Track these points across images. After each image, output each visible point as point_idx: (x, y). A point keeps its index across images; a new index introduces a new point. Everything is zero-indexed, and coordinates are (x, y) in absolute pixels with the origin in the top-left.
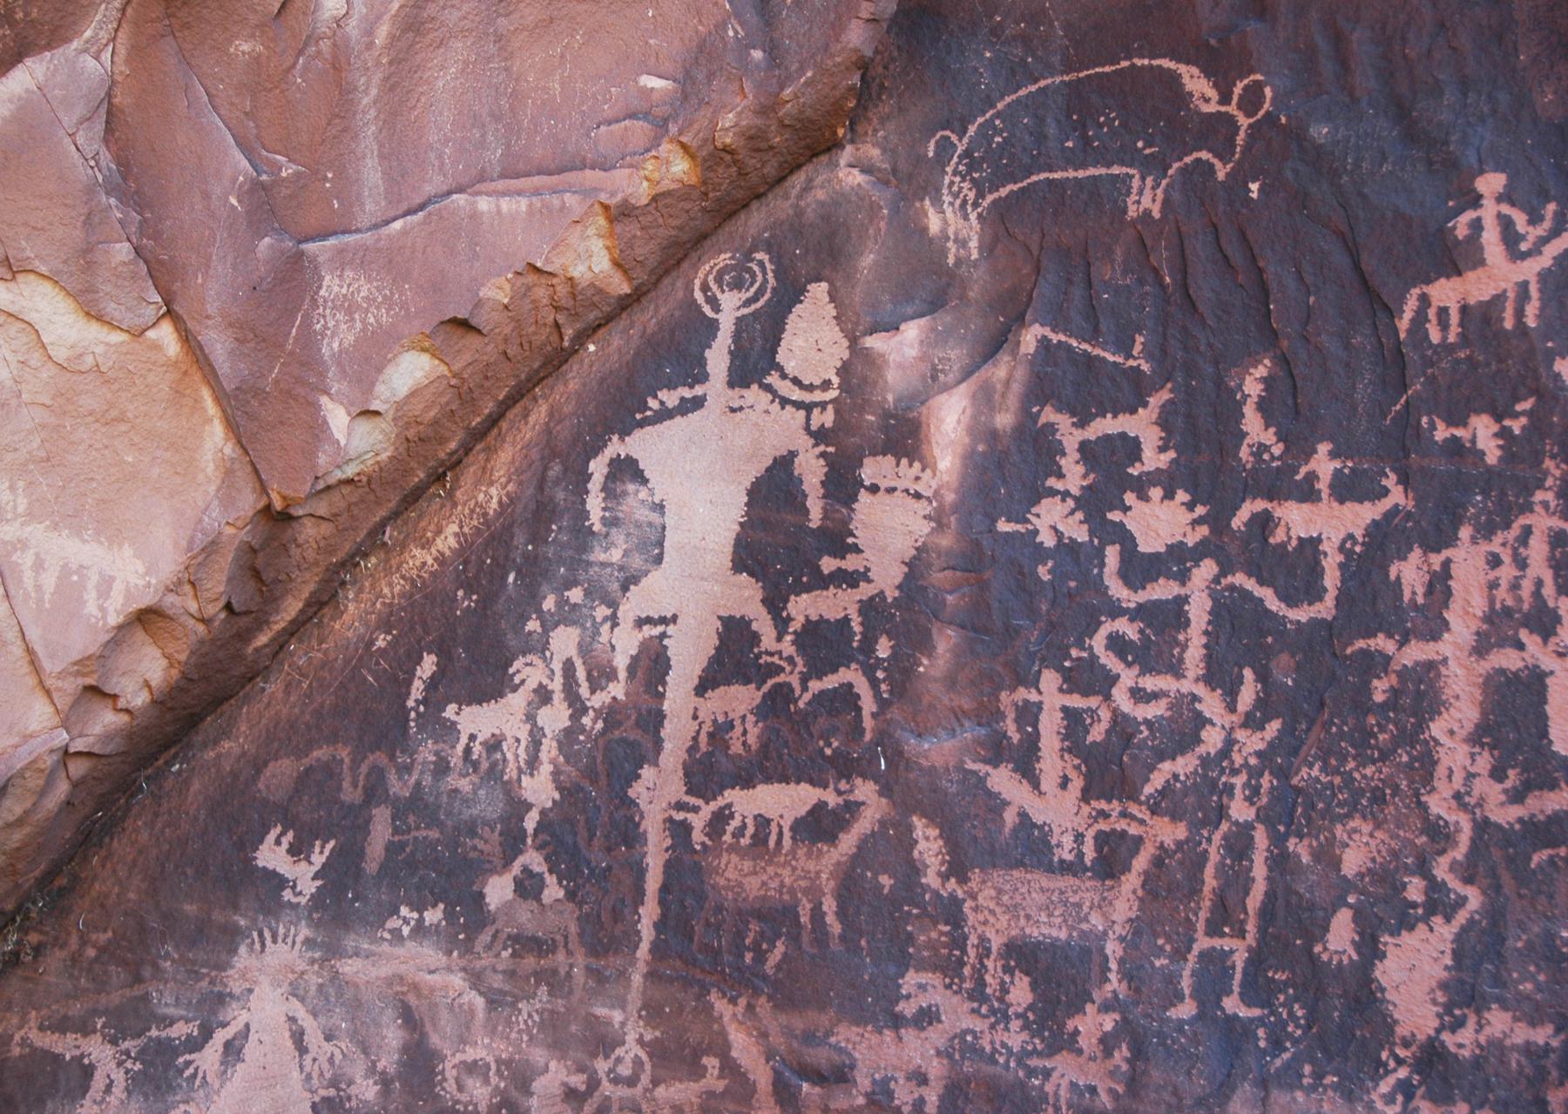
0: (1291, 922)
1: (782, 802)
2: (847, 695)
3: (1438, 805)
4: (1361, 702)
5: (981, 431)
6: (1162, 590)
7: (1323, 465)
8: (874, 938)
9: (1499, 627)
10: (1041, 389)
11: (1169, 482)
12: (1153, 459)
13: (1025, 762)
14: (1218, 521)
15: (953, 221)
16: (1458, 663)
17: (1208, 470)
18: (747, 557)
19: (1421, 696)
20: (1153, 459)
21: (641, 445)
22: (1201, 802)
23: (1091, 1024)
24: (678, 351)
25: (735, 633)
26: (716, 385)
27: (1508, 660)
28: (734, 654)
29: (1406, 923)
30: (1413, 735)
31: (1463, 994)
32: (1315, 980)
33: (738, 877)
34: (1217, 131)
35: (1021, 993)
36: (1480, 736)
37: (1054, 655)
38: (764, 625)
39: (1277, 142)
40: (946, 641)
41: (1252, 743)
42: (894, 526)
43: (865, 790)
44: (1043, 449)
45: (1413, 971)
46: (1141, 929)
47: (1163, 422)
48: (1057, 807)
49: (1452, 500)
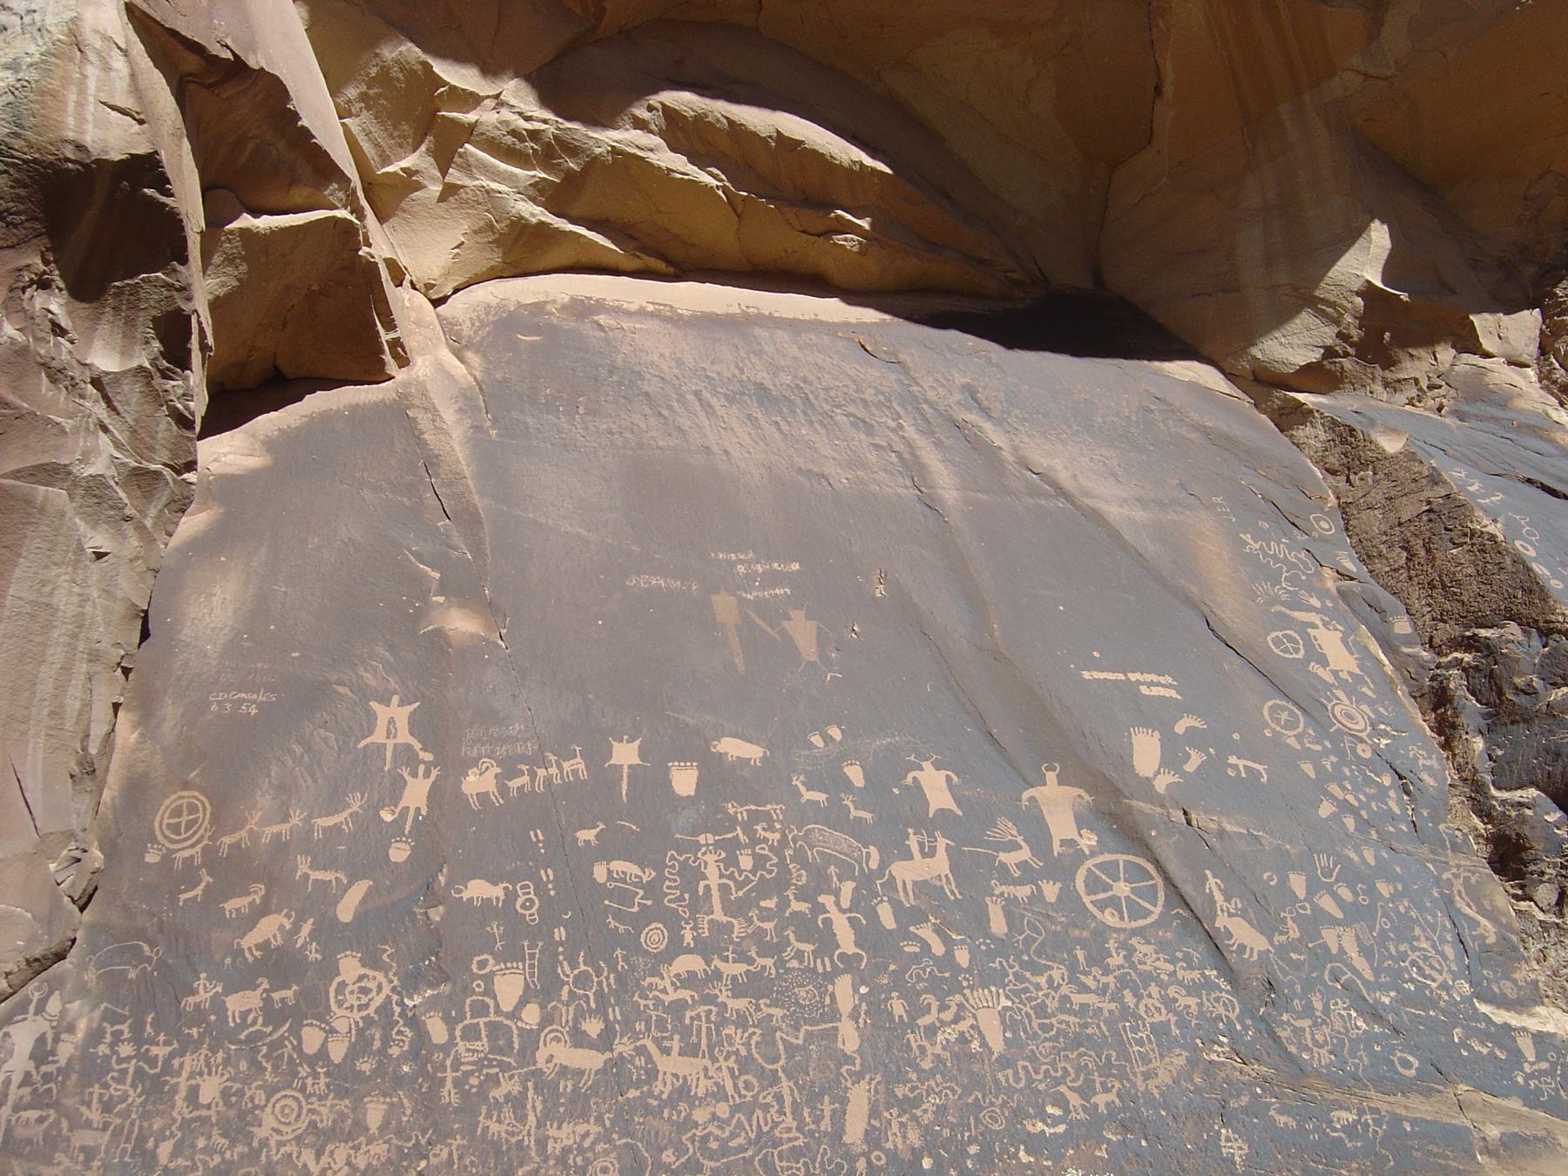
0: (142, 1139)
1: (33, 1114)
2: (50, 1090)
3: (174, 1114)
4: (162, 1092)
5: (89, 1028)
6: (124, 1066)
7: (162, 1038)
8: (54, 1142)
9: (192, 1075)
10: (104, 1019)
11: (129, 1041)
12: (126, 1035)
13: (89, 1104)
14: (138, 1050)
15: (91, 976)
16: (183, 1083)
17: (138, 1038)
18: (33, 1056)
19: (174, 1090)
20: (126, 1035)
21: (11, 1029)
22: (125, 1114)
23: (96, 1164)
24: (22, 1008)
25: (28, 1074)
26: (30, 1015)
27: (193, 1082)
28: (27, 1080)
29: (164, 1139)
30: (171, 1099)
31: (174, 1155)
32: (144, 1153)
33: (21, 1132)
34: (149, 959)
35: (81, 1157)
36: (187, 1099)
37: (98, 1080)
38: (34, 1073)
39: (162, 963)
40: (74, 1077)
41: (139, 1100)
42: (65, 1051)
43: (52, 1112)
44: (102, 1032)
45: (164, 1150)
46: (110, 1143)
47: (130, 1026)
48: (95, 1115)
49: (188, 1045)
